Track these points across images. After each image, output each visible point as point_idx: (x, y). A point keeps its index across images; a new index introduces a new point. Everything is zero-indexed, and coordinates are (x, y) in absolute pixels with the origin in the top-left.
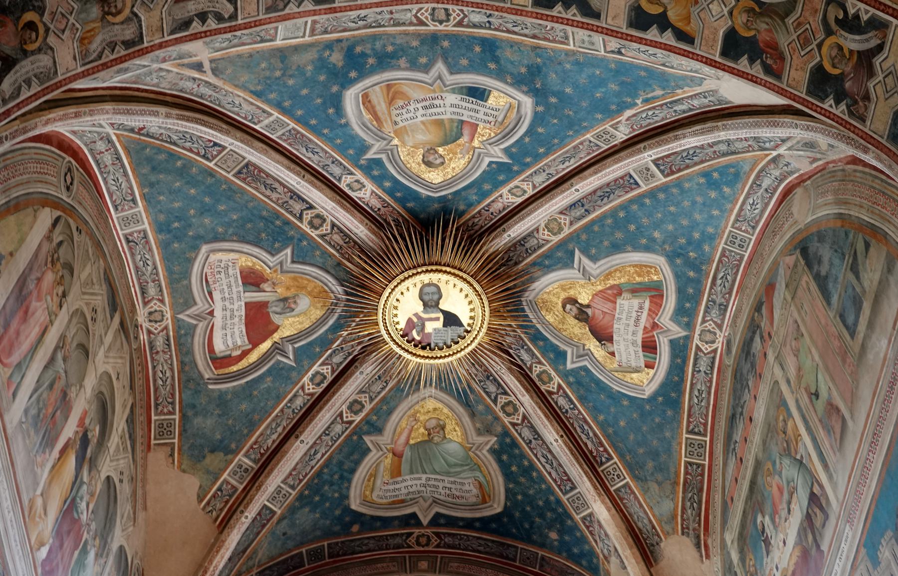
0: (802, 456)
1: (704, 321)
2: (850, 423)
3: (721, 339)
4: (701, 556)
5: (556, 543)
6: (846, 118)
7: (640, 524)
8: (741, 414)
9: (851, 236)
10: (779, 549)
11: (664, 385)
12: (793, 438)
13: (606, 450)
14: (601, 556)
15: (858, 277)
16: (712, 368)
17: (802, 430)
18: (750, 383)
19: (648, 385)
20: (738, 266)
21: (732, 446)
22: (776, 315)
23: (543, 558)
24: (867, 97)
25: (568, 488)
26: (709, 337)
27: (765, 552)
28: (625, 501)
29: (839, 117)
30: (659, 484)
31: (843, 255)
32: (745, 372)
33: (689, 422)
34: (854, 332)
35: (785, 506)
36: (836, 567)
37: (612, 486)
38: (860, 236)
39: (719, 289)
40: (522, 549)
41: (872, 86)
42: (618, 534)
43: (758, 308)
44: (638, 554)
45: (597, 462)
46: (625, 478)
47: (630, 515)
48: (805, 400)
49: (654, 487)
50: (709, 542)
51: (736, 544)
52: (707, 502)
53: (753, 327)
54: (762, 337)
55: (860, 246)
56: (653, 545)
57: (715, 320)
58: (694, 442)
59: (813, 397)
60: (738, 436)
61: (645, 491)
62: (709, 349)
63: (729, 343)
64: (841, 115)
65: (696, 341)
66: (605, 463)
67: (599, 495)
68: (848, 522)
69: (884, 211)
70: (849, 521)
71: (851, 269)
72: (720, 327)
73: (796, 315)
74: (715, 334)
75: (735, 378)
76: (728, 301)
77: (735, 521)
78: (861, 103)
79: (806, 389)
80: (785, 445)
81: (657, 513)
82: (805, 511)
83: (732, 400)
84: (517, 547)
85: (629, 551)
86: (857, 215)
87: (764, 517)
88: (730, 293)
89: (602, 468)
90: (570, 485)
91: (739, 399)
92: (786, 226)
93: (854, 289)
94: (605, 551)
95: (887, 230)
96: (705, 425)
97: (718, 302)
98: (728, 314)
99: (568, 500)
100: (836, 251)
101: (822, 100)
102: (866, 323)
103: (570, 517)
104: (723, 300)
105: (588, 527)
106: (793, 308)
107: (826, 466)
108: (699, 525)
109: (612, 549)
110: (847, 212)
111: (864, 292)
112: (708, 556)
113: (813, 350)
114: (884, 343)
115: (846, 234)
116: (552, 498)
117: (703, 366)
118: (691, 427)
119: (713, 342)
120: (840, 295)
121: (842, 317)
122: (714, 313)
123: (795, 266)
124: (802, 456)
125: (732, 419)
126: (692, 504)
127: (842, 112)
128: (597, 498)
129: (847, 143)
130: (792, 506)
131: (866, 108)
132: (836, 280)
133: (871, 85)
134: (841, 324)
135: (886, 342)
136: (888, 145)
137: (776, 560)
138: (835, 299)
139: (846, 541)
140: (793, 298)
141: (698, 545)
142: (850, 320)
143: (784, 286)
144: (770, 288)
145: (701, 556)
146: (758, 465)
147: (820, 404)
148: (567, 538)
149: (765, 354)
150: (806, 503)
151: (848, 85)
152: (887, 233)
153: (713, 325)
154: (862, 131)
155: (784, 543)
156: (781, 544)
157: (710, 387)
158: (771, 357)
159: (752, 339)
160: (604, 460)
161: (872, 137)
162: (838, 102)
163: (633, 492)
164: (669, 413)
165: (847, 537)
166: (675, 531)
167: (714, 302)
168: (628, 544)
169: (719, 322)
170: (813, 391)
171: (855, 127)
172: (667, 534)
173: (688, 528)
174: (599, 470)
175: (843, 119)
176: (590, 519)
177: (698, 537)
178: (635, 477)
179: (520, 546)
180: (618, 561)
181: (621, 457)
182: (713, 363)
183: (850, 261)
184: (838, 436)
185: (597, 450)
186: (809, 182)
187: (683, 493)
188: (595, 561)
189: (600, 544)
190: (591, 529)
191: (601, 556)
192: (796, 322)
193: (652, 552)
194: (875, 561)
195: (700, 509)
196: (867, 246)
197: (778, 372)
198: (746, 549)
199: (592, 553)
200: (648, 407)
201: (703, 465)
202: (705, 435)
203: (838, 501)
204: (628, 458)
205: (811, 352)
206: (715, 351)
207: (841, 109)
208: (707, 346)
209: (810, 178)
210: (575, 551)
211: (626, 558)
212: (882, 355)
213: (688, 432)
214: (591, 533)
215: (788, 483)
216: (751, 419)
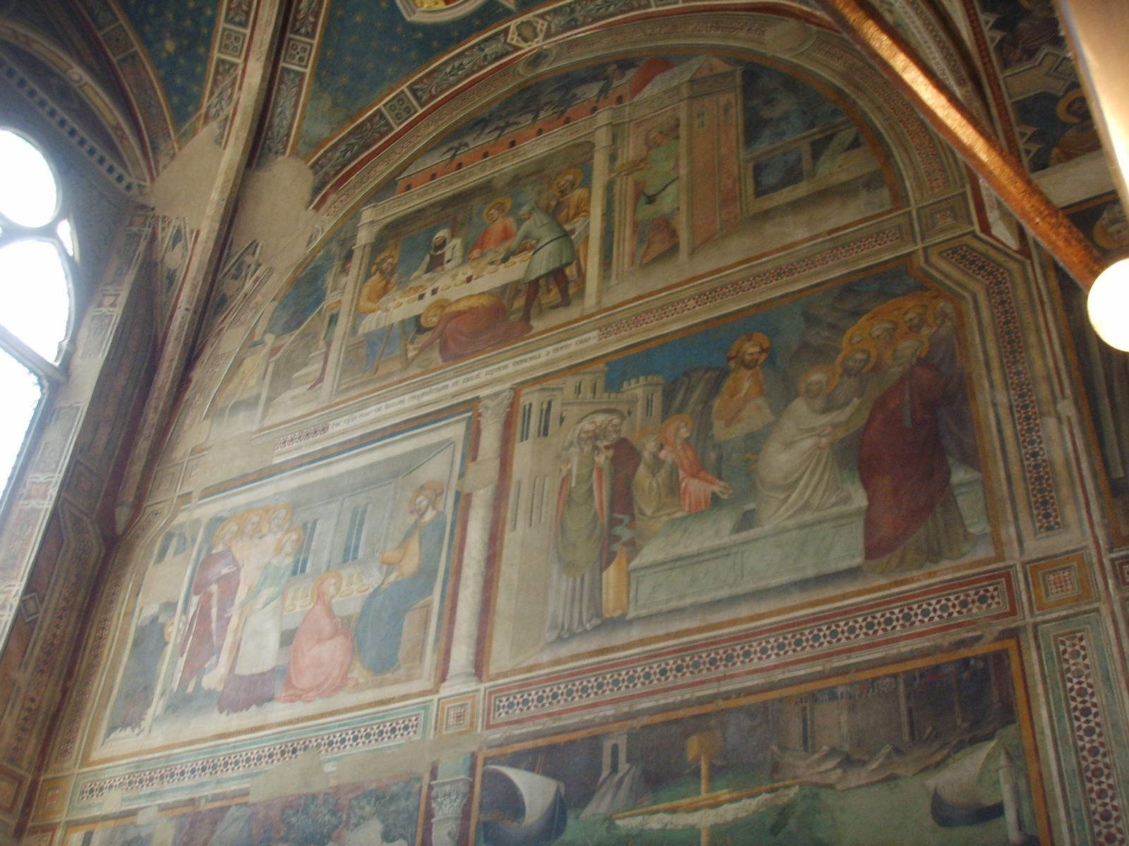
0: (573, 231)
1: (542, 16)
2: (683, 257)
3: (534, 46)
4: (311, 202)
5: (164, 55)
6: (991, 47)
7: (276, 120)
8: (503, 129)
9: (839, 120)
10: (454, 277)
11: (437, 27)
12: (573, 205)
13: (315, 25)
14: (203, 110)
15: (816, 154)
16: (497, 59)
17: (597, 210)
18: (542, 115)
19: (423, 12)
20: (632, 9)
21: (456, 144)
22: (647, 92)
23: (134, 55)
24: (1031, 54)
25: (237, 19)
26: (527, 32)
27: (424, 265)
28: (283, 87)
29: (983, 37)
30: (335, 104)
31: (812, 125)
32: (544, 99)
33: (420, 81)
34: (764, 193)
35: (502, 250)
36: (543, 352)
37: (284, 61)
38: (854, 130)
39: (592, 7)
40: (121, 26)
41: (1046, 51)
42: (250, 111)
43: (624, 64)
44: (251, 144)
45: (294, 26)
46: (306, 67)
47: (276, 103)
48: (626, 187)
49: (326, 102)
50: (332, 197)
51: (377, 228)
52: (362, 163)
53: (597, 72)
54: (604, 91)
55: (846, 136)
56: (270, 150)
57: (553, 26)
58: (406, 101)
59: (643, 199)
60: (476, 142)
61: (313, 97)
62: (514, 42)
63: (537, 58)
64: (988, 40)
65: (513, 24)
66: (300, 34)
67: (268, 58)
68: (600, 329)
69: (909, 138)
70: (605, 330)
71: (813, 144)
72: (548, 35)
73: (683, 114)
74: (536, 36)
75: (522, 91)
76: (583, 25)
77: (395, 208)
78: (1018, 51)
79: (637, 184)
80: (553, 203)
81: (305, 126)
82: (533, 277)
83: (494, 107)
84: (116, 19)
85: (245, 135)
86: (866, 109)
87: (453, 236)
88: (594, 21)
89: (292, 36)
90: (243, 18)
91: (511, 114)
92: (741, 34)
93: (799, 160)
94: (213, 111)
95: (895, 153)
96: (432, 98)
97: (576, 15)
98: (569, 34)
99: (224, 29)
100: (804, 113)
101: (985, 9)
102: (789, 199)
103: (208, 47)
104: (581, 19)
105: (217, 73)
106: (683, 105)
107: (606, 262)
108: (336, 174)
109: (222, 116)
110: (853, 96)
111: (813, 173)
112: (317, 208)
113: (683, 162)
114: (801, 234)
115: (834, 113)
116: (209, 12)
117: (490, 50)
118: (417, 87)
119: (525, 40)
120: (774, 150)
121: (758, 170)
122: (560, 20)
123: (724, 75)
124: (573, 231)
125: (478, 123)
126: (347, 151)
127: (993, 40)
128: (263, 58)
129: (945, 58)
130: (517, 259)
131: (1019, 61)
132: (780, 134)
133: (1046, 49)
134: (750, 173)
135: (807, 235)
136: (1010, 110)
137: (440, 284)
138: (762, 147)
139: (581, 342)
140: (691, 98)
141: (316, 190)
142: (769, 179)
143: (687, 77)
144: (660, 63)
145: (311, 202)
146: (485, 189)
147: (647, 211)
148: (182, 61)
149: (594, 110)
150: (542, 272)
151: (1023, 25)
152: (892, 156)
153: (544, 28)
154: (994, 71)
155: (469, 280)
156: (462, 278)
157: (474, 72)
158: (603, 117)
159: (583, 81)
160: (303, 30)
161: (999, 86)
162: (997, 26)
163: (300, 87)
164: (413, 55)
165: (586, 340)
166: (306, 158)
167: (572, 11)
168: (250, 129)
169: (553, 31)
170: (650, 191)
171: (990, 61)
172: (295, 153)
173: (322, 167)
174: (289, 35)
175: (985, 43)
176: (225, 68)
177: (324, 184)
178: (317, 75)
179: (122, 21)
180: (218, 132)
181: (324, 46)
182: (503, 56)
183: (816, 137)
184: (652, 255)
185: (306, 16)
186: (814, 28)
187: (350, 133)
188: (191, 108)
189: (214, 100)
190: (219, 77)
191: (203, 110)
192: (678, 120)
193: (261, 155)
194: (613, 384)
195: (350, 161)
196: (855, 144)
197: (602, 139)
198: (391, 242)
199: (196, 100)
200: (399, 30)
201: (392, 129)
202: (422, 107)
203: (599, 302)
204: (329, 53)
205: (677, 159)
206: (517, 49)
207: (995, 35)
208: (515, 37)
209: (819, 25)
210: (178, 81)
211: (237, 138)
212: (789, 240)
213: (410, 88)
214: (215, 82)
215: (527, 236)
216: (512, 144)
